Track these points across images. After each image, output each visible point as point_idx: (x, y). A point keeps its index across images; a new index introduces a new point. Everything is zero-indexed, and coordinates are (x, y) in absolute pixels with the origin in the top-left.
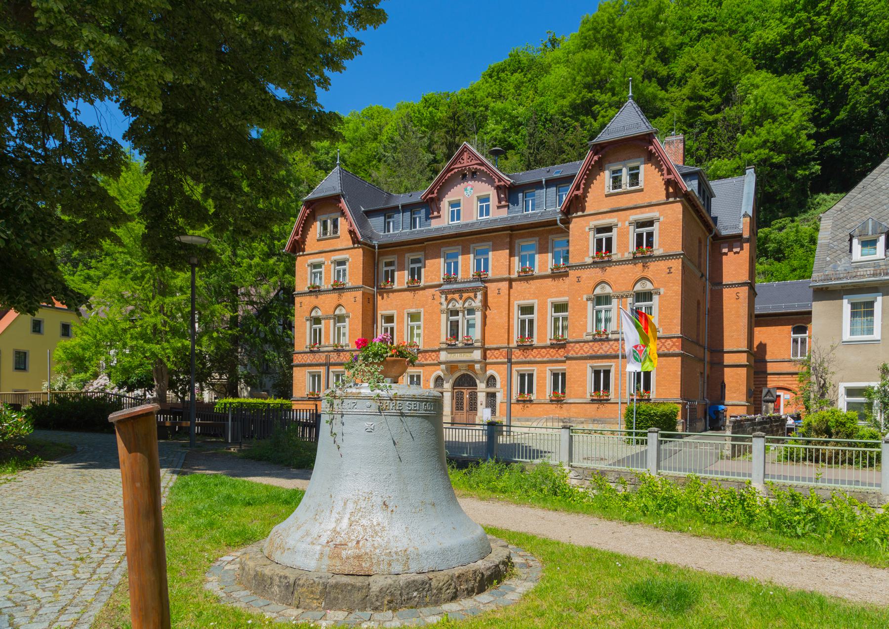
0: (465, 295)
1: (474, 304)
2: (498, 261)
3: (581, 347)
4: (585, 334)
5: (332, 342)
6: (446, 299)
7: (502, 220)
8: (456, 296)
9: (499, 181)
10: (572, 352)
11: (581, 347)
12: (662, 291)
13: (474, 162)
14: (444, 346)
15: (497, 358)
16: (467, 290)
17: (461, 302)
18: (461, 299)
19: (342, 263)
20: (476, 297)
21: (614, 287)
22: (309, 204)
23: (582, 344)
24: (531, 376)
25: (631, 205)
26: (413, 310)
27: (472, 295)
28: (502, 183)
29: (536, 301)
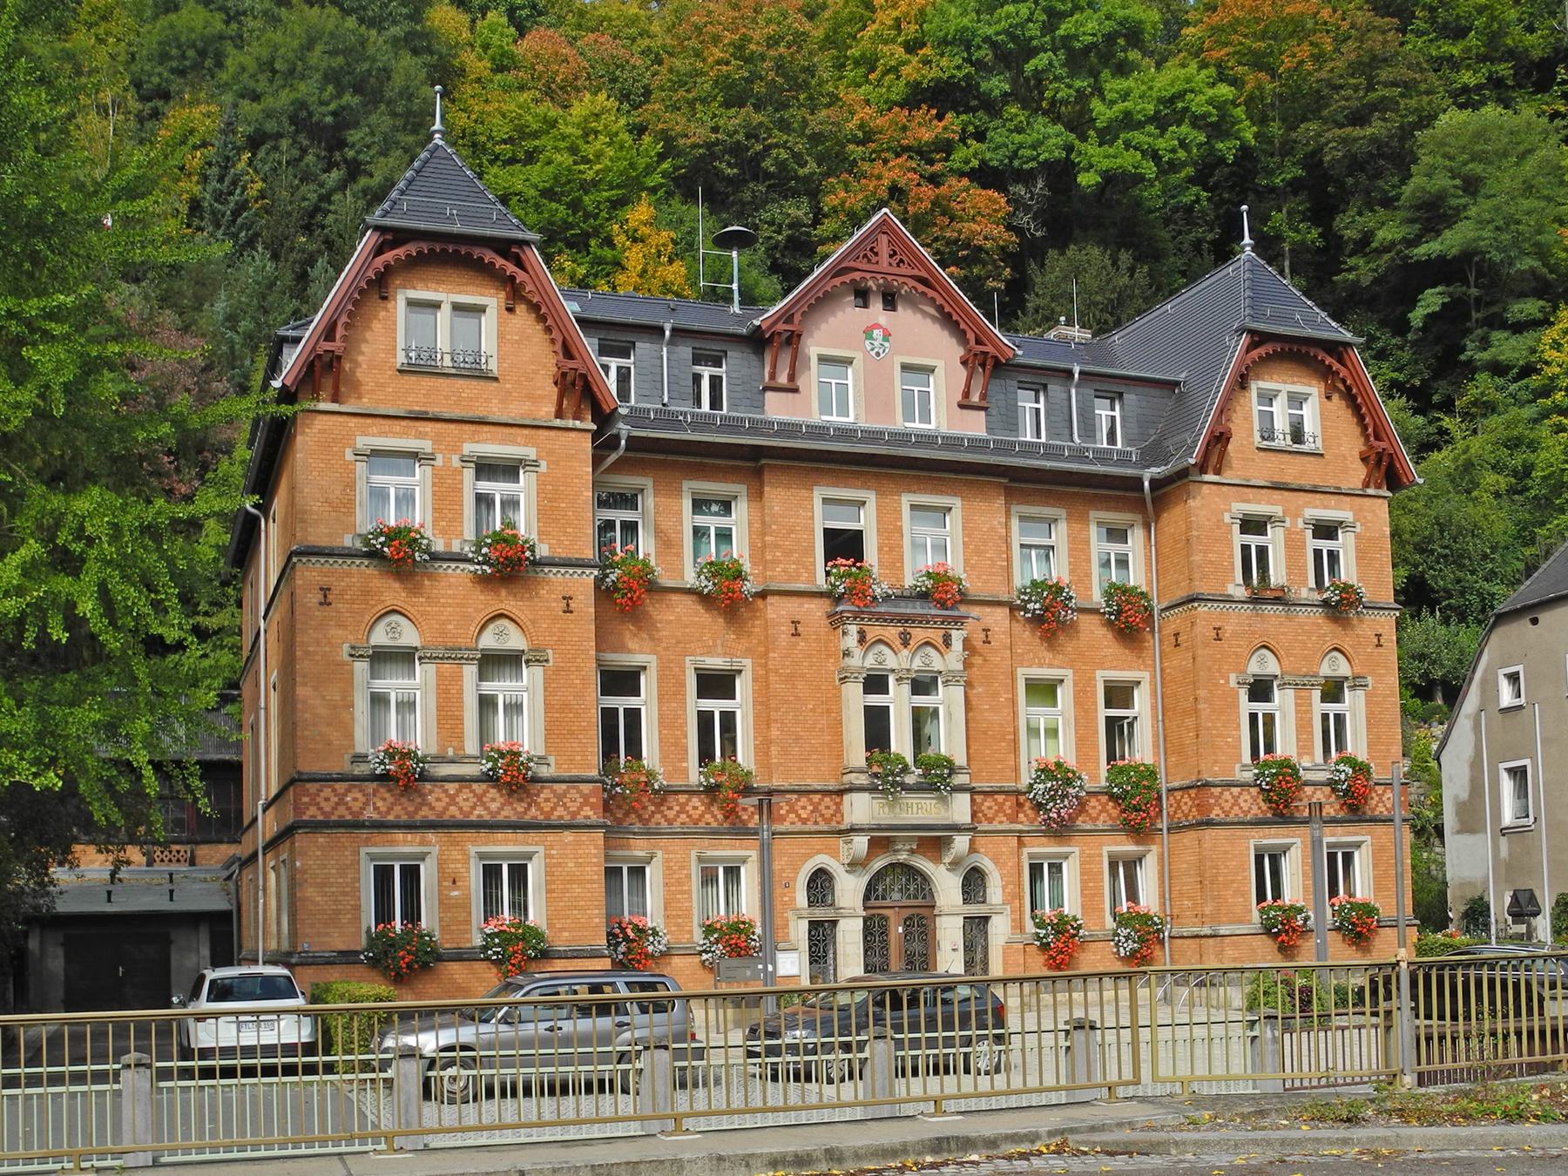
0: (919, 634)
1: (937, 663)
2: (978, 552)
3: (1236, 798)
4: (1238, 766)
5: (471, 747)
6: (862, 639)
7: (952, 442)
8: (892, 633)
9: (978, 342)
10: (1216, 811)
11: (1236, 798)
12: (1370, 680)
13: (904, 270)
14: (863, 780)
15: (990, 820)
16: (922, 621)
17: (905, 652)
18: (906, 644)
19: (1326, 530)
20: (947, 641)
21: (1285, 662)
22: (393, 237)
23: (1236, 790)
24: (411, 875)
25: (1306, 482)
26: (716, 662)
27: (936, 636)
28: (989, 349)
29: (1069, 672)
